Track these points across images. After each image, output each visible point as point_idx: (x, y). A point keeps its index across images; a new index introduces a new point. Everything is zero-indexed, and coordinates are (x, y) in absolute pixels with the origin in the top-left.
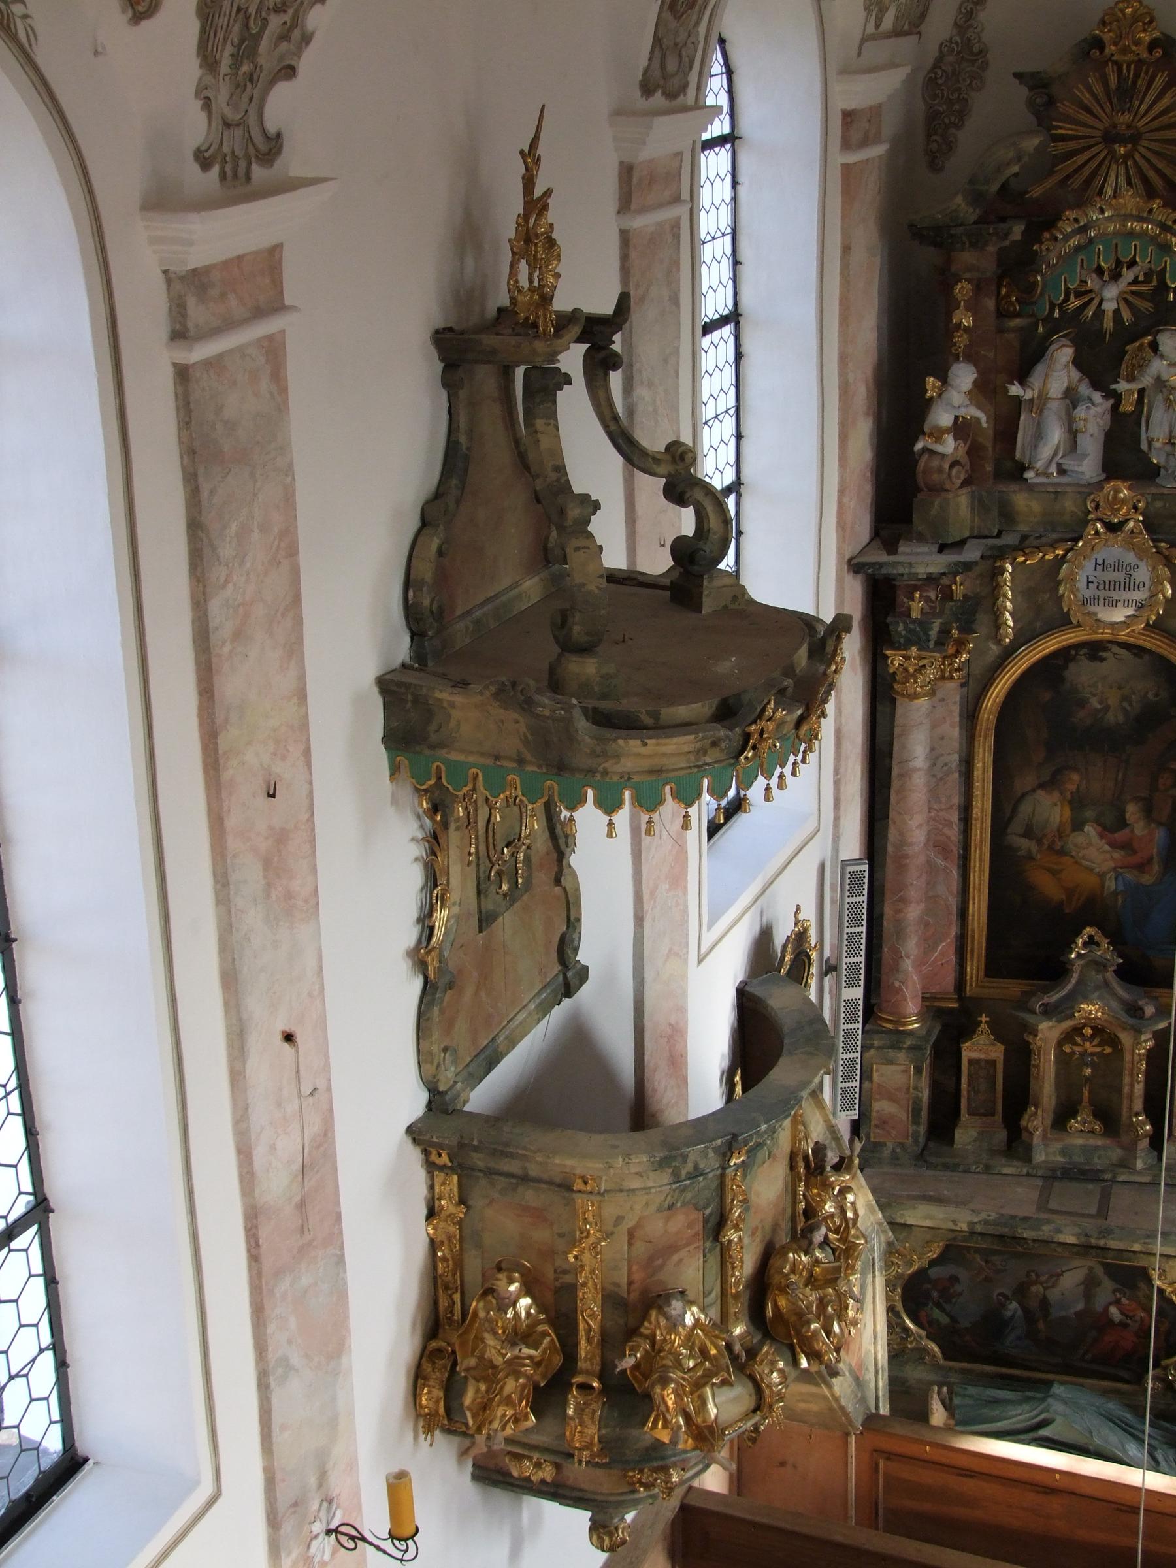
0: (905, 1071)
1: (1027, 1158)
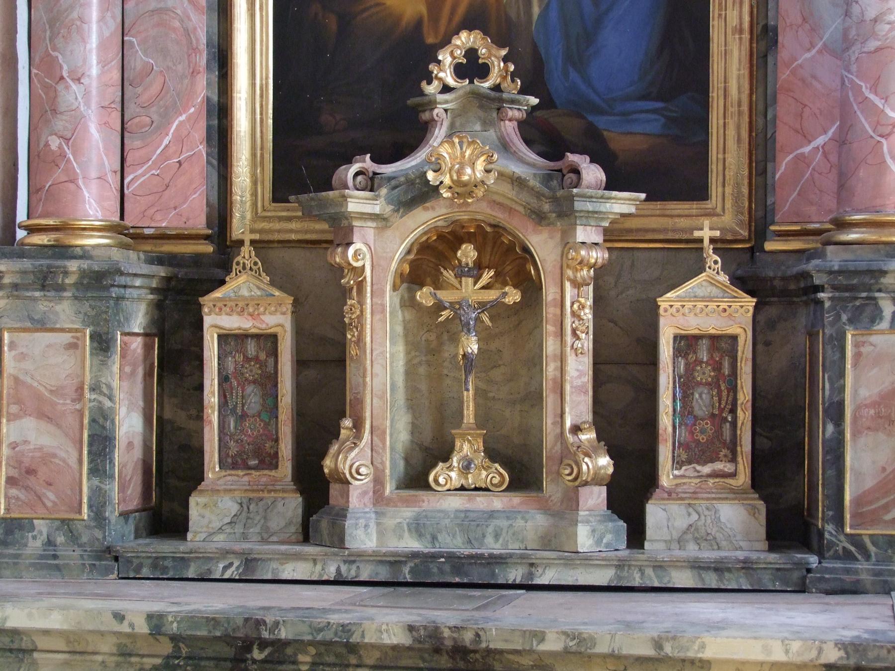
0: (72, 346)
1: (338, 540)
